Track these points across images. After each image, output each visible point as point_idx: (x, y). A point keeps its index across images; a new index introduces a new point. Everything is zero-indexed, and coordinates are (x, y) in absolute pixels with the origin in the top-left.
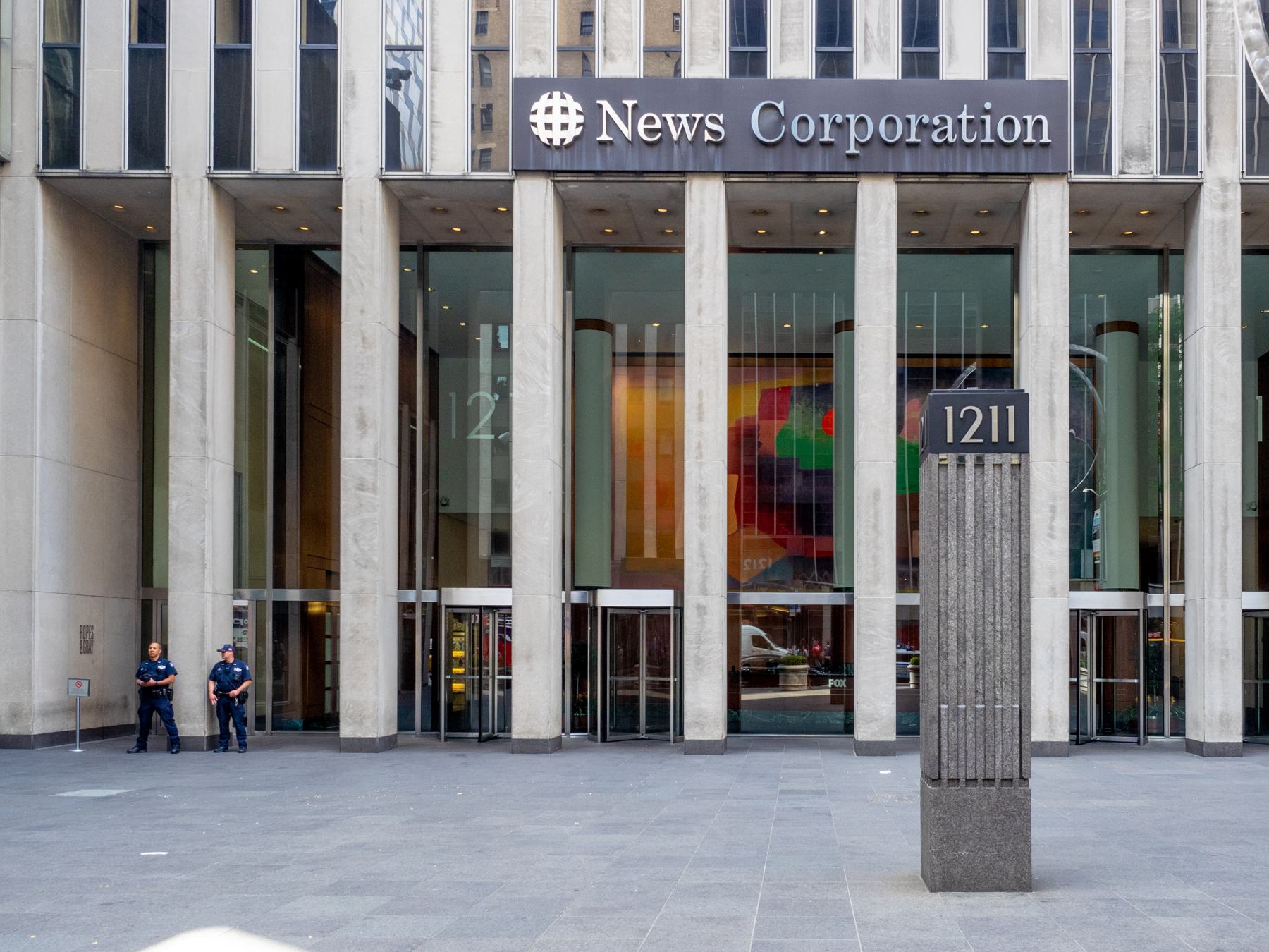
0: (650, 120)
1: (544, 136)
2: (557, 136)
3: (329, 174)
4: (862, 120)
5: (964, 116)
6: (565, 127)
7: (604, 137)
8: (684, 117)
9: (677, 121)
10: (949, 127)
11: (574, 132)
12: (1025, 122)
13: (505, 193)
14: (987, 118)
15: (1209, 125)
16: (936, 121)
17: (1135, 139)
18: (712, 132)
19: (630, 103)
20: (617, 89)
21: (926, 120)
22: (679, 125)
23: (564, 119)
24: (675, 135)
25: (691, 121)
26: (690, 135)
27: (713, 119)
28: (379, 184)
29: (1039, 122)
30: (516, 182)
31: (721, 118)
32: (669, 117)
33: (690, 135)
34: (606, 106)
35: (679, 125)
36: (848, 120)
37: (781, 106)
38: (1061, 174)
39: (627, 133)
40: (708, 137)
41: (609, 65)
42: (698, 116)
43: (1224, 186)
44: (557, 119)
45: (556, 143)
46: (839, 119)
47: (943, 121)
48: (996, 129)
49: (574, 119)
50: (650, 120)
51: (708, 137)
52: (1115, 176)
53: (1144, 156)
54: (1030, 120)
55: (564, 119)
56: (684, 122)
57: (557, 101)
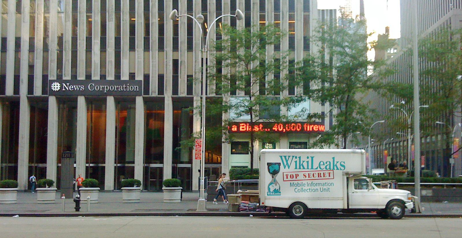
0: (71, 87)
1: (54, 89)
2: (56, 89)
3: (18, 96)
4: (107, 87)
5: (124, 86)
6: (57, 88)
7: (64, 90)
8: (77, 86)
9: (76, 87)
10: (122, 88)
11: (59, 89)
12: (134, 87)
13: (46, 100)
14: (128, 87)
15: (166, 87)
16: (119, 87)
17: (154, 90)
18: (82, 89)
19: (68, 84)
20: (66, 82)
21: (118, 87)
22: (76, 88)
23: (57, 87)
24: (76, 89)
25: (78, 87)
26: (78, 89)
27: (82, 87)
28: (26, 98)
29: (137, 87)
30: (49, 97)
31: (83, 86)
32: (75, 86)
33: (78, 89)
34: (64, 85)
35: (76, 88)
36: (104, 87)
37: (93, 85)
38: (140, 95)
39: (67, 89)
40: (81, 90)
41: (65, 78)
42: (79, 86)
43: (168, 97)
44: (56, 87)
45: (56, 91)
46: (103, 87)
47: (121, 87)
48: (129, 88)
49: (59, 87)
50: (71, 87)
51: (81, 90)
52: (150, 96)
53: (155, 92)
54: (135, 87)
55: (57, 87)
56: (77, 87)
57: (56, 84)
